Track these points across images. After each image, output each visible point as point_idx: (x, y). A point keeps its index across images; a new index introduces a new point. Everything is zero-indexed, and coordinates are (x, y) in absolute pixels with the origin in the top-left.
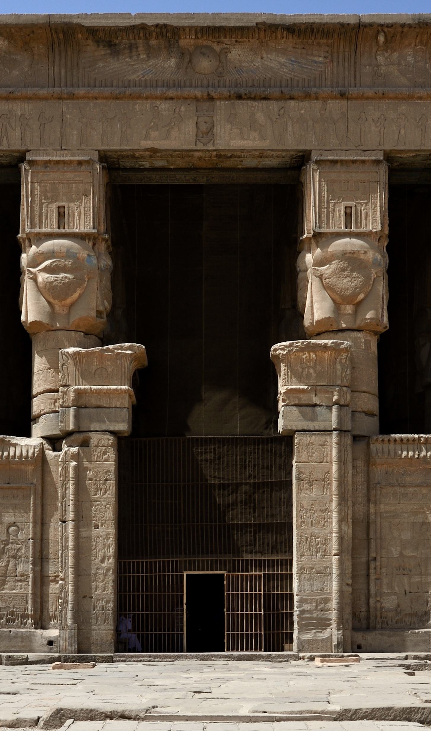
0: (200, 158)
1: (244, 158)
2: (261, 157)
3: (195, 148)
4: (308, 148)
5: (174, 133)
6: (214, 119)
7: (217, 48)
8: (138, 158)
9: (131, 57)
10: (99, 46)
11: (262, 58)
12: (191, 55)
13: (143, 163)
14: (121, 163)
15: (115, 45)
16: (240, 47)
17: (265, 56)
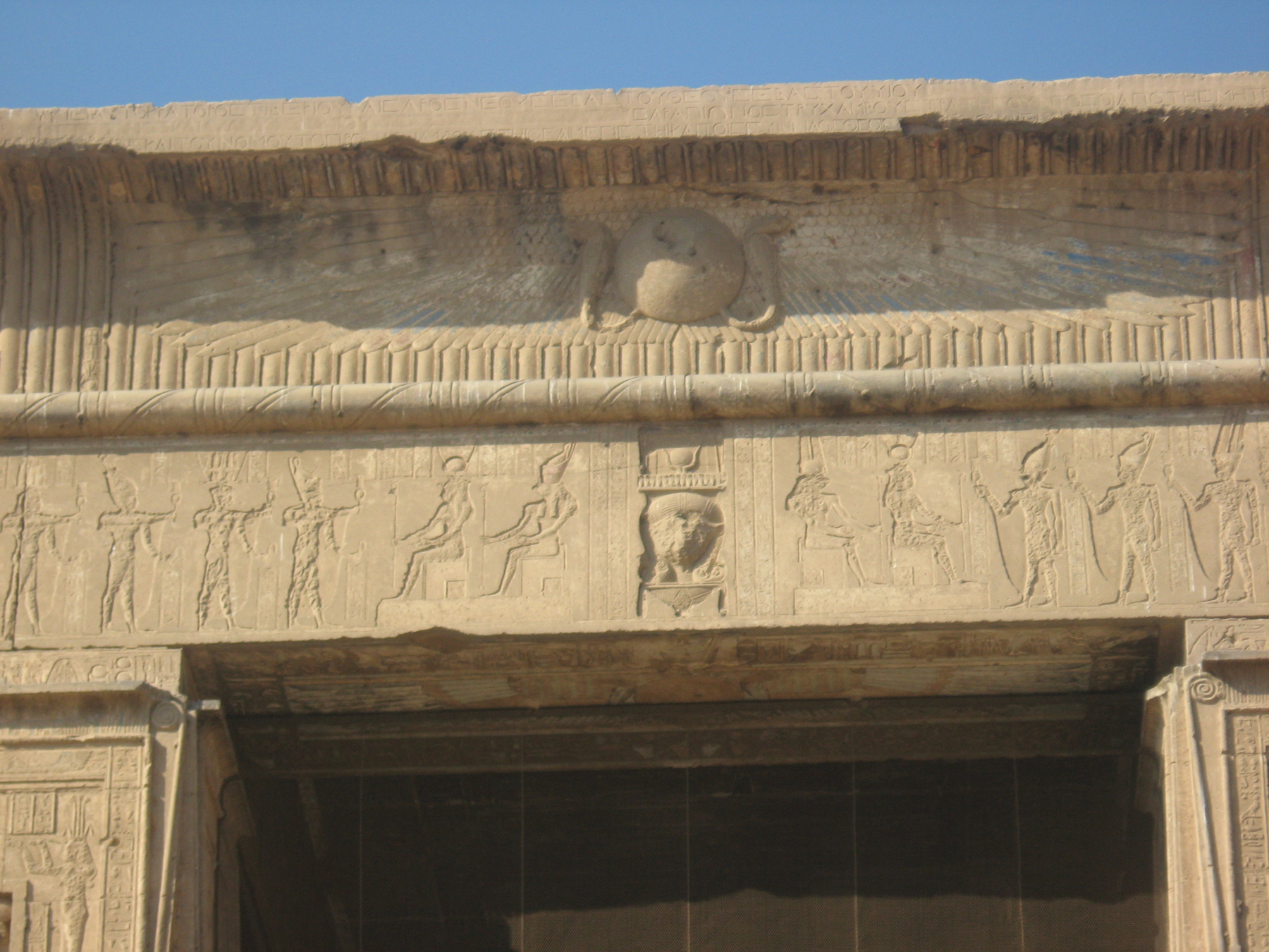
0: (662, 666)
1: (869, 656)
2: (950, 653)
3: (633, 624)
4: (1169, 611)
5: (535, 567)
6: (721, 502)
7: (734, 218)
8: (373, 670)
9: (345, 264)
10: (202, 225)
11: (936, 250)
12: (612, 249)
13: (397, 691)
14: (292, 693)
15: (276, 218)
16: (834, 209)
17: (948, 239)
